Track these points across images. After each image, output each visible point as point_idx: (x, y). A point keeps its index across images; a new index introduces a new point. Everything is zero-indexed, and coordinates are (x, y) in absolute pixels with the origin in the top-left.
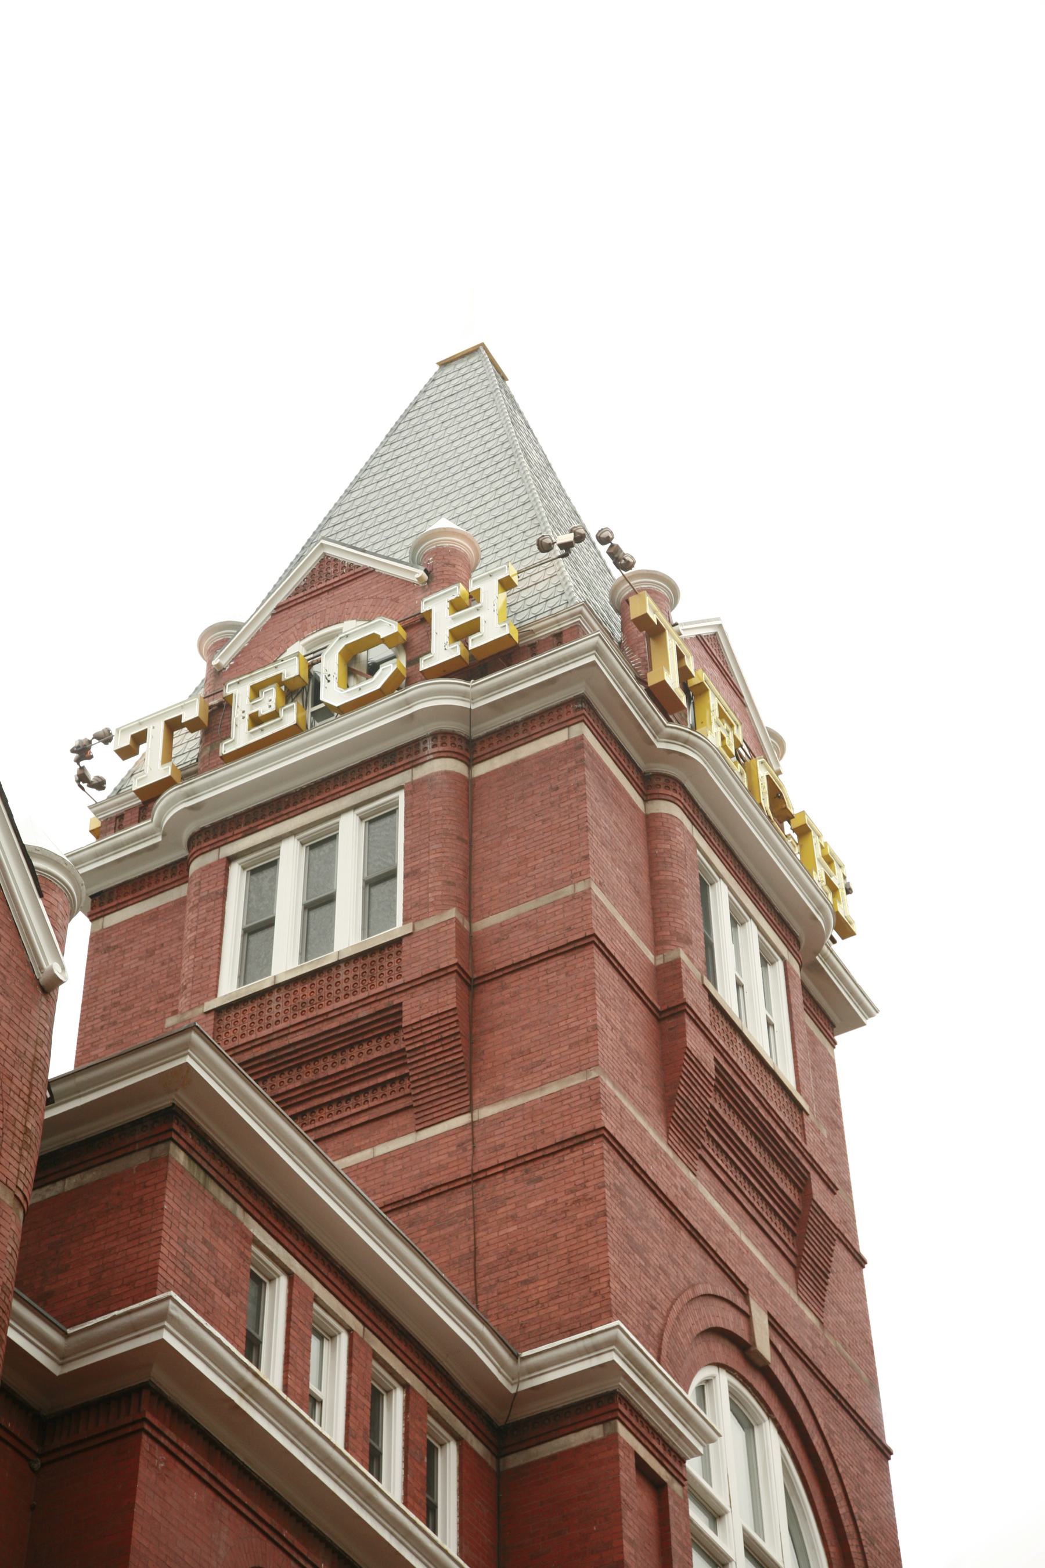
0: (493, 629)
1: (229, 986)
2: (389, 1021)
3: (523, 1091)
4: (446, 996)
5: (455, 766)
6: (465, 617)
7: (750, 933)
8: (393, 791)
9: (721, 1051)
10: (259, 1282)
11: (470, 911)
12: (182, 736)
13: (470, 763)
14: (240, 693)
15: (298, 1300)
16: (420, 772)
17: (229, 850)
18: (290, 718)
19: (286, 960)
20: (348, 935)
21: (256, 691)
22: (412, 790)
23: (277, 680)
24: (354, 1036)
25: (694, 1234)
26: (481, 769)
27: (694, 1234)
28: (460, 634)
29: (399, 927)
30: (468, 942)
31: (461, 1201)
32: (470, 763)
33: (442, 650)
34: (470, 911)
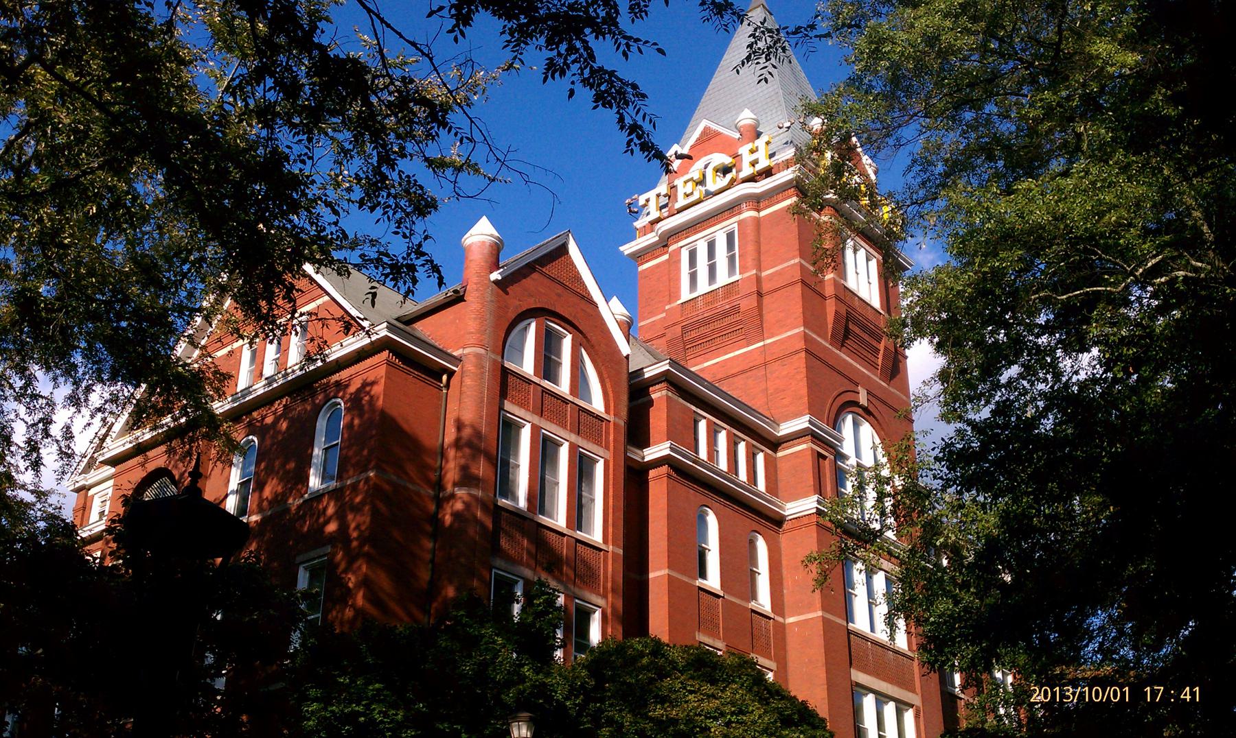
0: (763, 163)
1: (685, 295)
2: (735, 310)
3: (781, 333)
4: (752, 302)
5: (753, 213)
6: (754, 157)
7: (862, 254)
8: (732, 223)
9: (849, 306)
10: (696, 422)
11: (760, 269)
12: (662, 198)
13: (758, 211)
14: (679, 182)
15: (709, 423)
16: (742, 216)
17: (681, 244)
18: (696, 196)
19: (703, 287)
20: (723, 278)
21: (686, 182)
22: (740, 223)
23: (692, 179)
24: (726, 314)
25: (839, 373)
26: (763, 213)
27: (839, 373)
28: (753, 164)
29: (737, 277)
30: (758, 279)
31: (762, 372)
32: (758, 211)
33: (747, 171)
34: (760, 269)
